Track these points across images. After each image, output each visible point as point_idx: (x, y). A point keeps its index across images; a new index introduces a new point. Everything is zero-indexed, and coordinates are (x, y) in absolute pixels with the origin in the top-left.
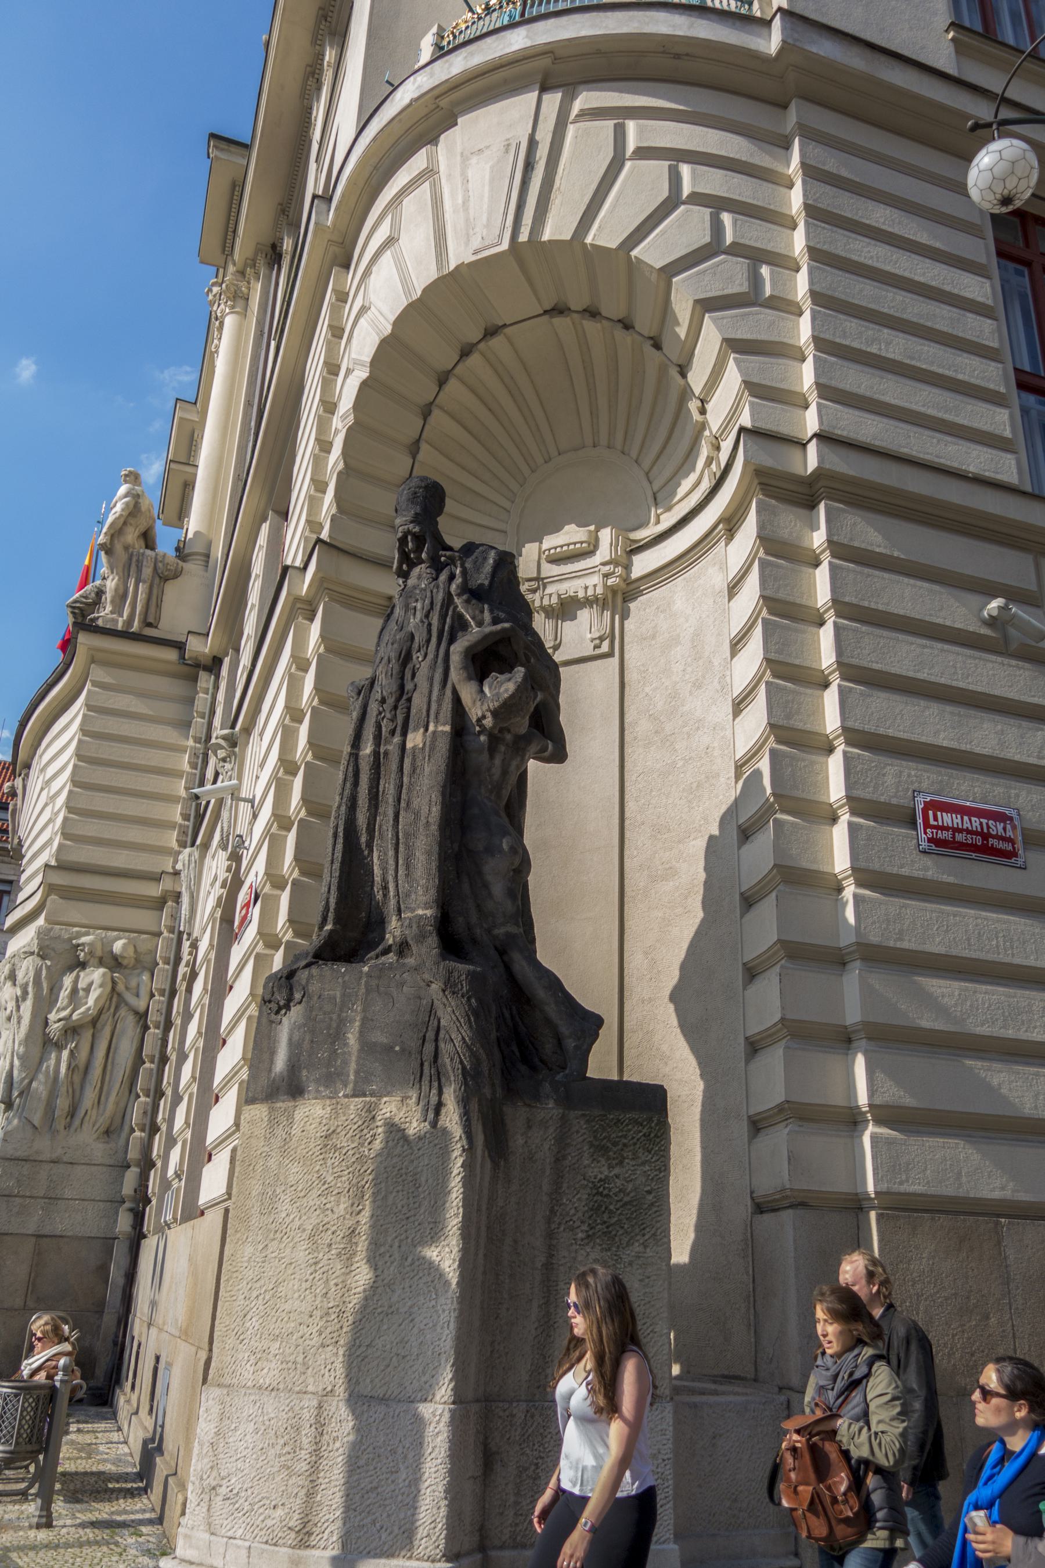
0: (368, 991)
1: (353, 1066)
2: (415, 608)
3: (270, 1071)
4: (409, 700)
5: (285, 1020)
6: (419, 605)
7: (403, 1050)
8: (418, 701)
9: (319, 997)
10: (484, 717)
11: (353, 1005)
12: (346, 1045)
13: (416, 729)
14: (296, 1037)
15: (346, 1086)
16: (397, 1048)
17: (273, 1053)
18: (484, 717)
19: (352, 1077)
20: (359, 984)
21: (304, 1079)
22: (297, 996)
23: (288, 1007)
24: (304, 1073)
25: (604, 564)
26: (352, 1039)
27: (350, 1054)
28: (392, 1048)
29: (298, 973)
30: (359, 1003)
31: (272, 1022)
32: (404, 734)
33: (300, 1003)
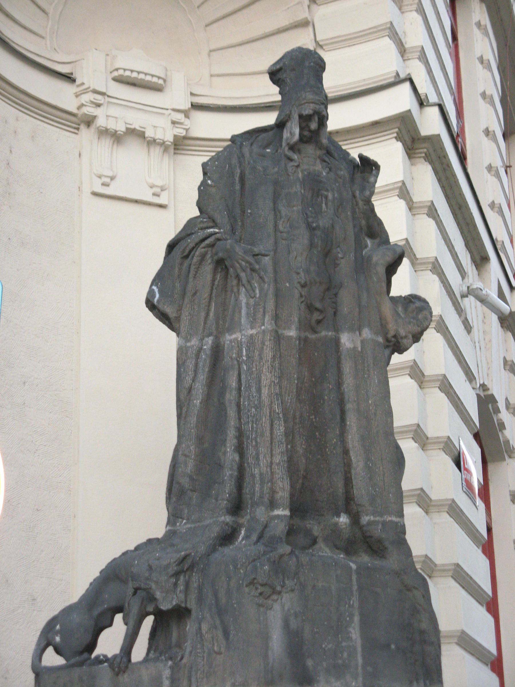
0: (361, 588)
1: (360, 660)
2: (326, 197)
3: (266, 656)
4: (336, 295)
5: (277, 607)
6: (330, 196)
7: (398, 648)
8: (346, 300)
9: (314, 587)
10: (406, 337)
11: (350, 600)
12: (350, 639)
13: (351, 330)
14: (294, 624)
15: (356, 679)
16: (393, 646)
17: (266, 638)
18: (406, 337)
19: (360, 670)
20: (351, 580)
21: (311, 668)
22: (289, 583)
23: (279, 593)
24: (310, 663)
25: (174, 110)
26: (355, 633)
27: (355, 649)
28: (388, 646)
29: (286, 558)
30: (354, 598)
31: (260, 605)
32: (337, 330)
33: (292, 591)
